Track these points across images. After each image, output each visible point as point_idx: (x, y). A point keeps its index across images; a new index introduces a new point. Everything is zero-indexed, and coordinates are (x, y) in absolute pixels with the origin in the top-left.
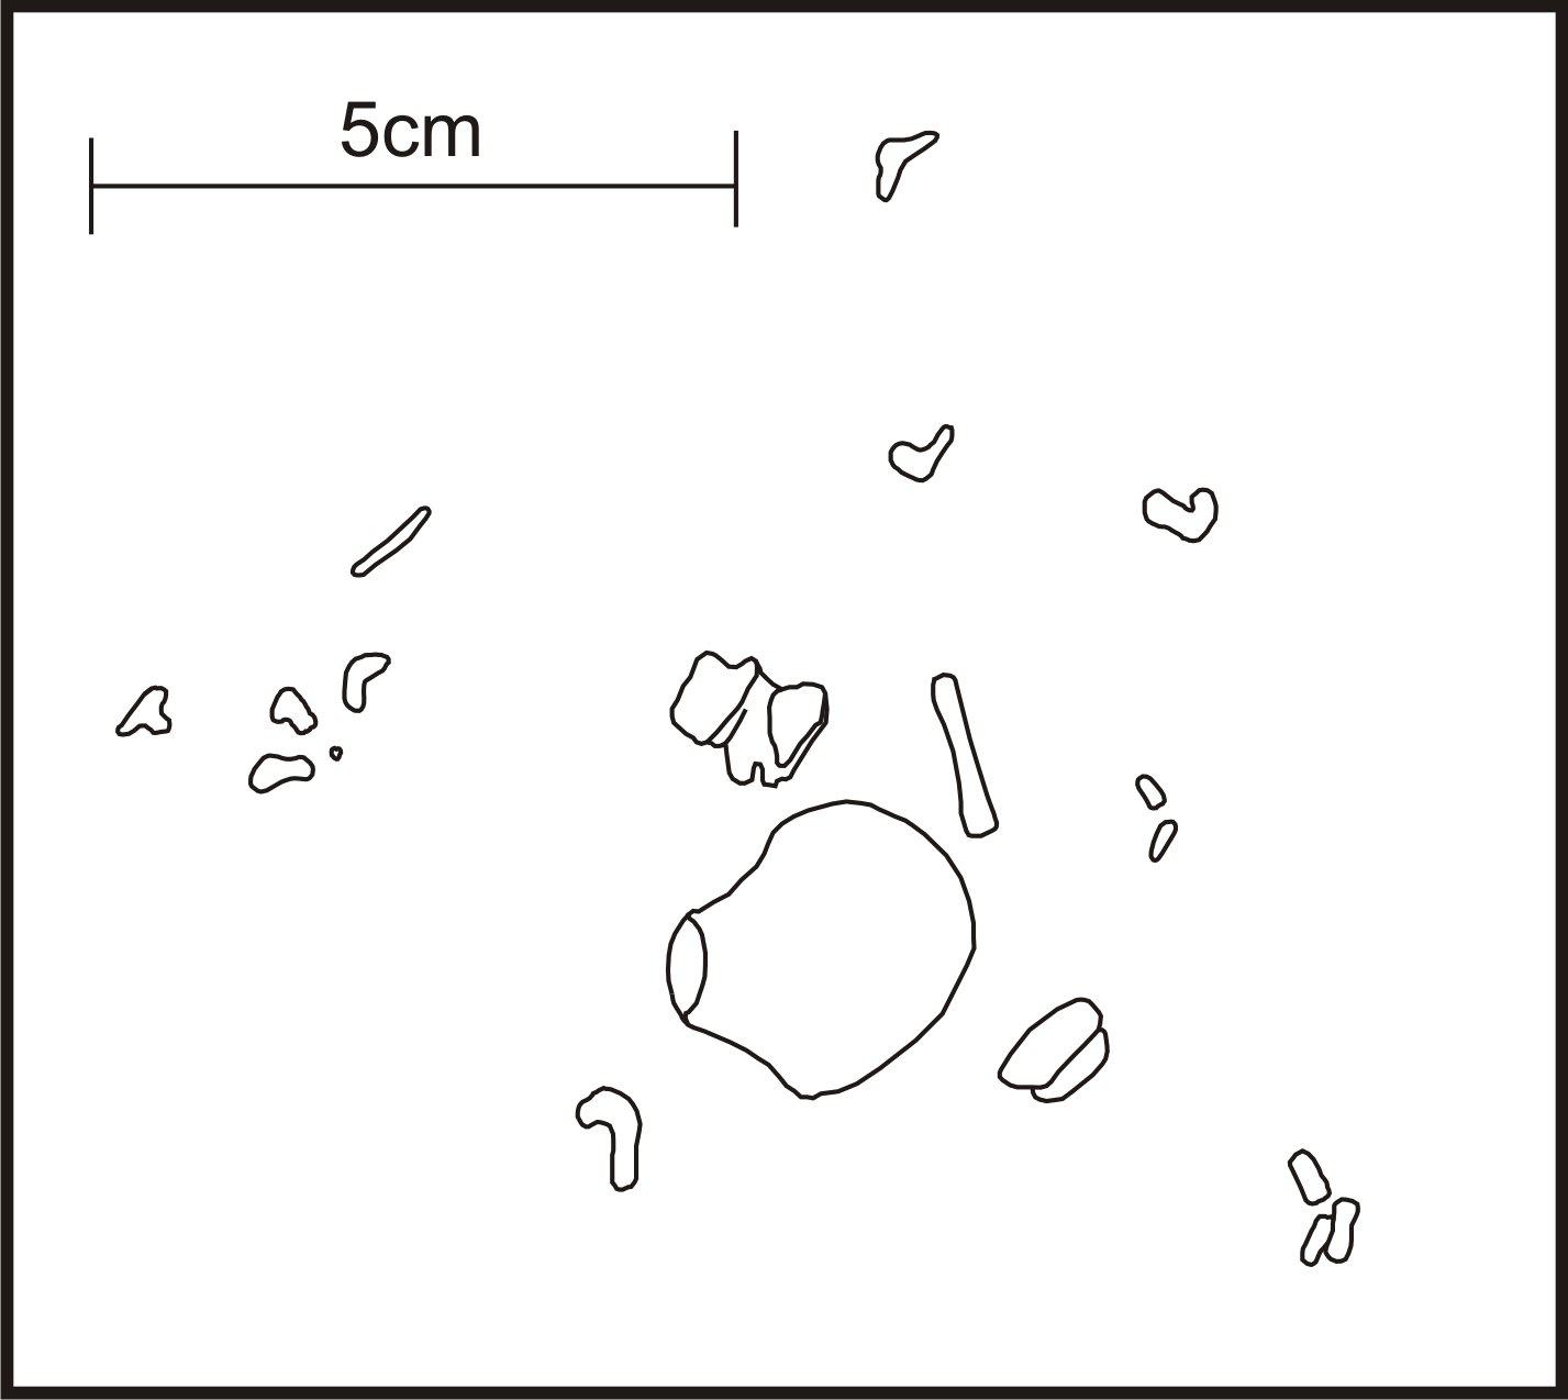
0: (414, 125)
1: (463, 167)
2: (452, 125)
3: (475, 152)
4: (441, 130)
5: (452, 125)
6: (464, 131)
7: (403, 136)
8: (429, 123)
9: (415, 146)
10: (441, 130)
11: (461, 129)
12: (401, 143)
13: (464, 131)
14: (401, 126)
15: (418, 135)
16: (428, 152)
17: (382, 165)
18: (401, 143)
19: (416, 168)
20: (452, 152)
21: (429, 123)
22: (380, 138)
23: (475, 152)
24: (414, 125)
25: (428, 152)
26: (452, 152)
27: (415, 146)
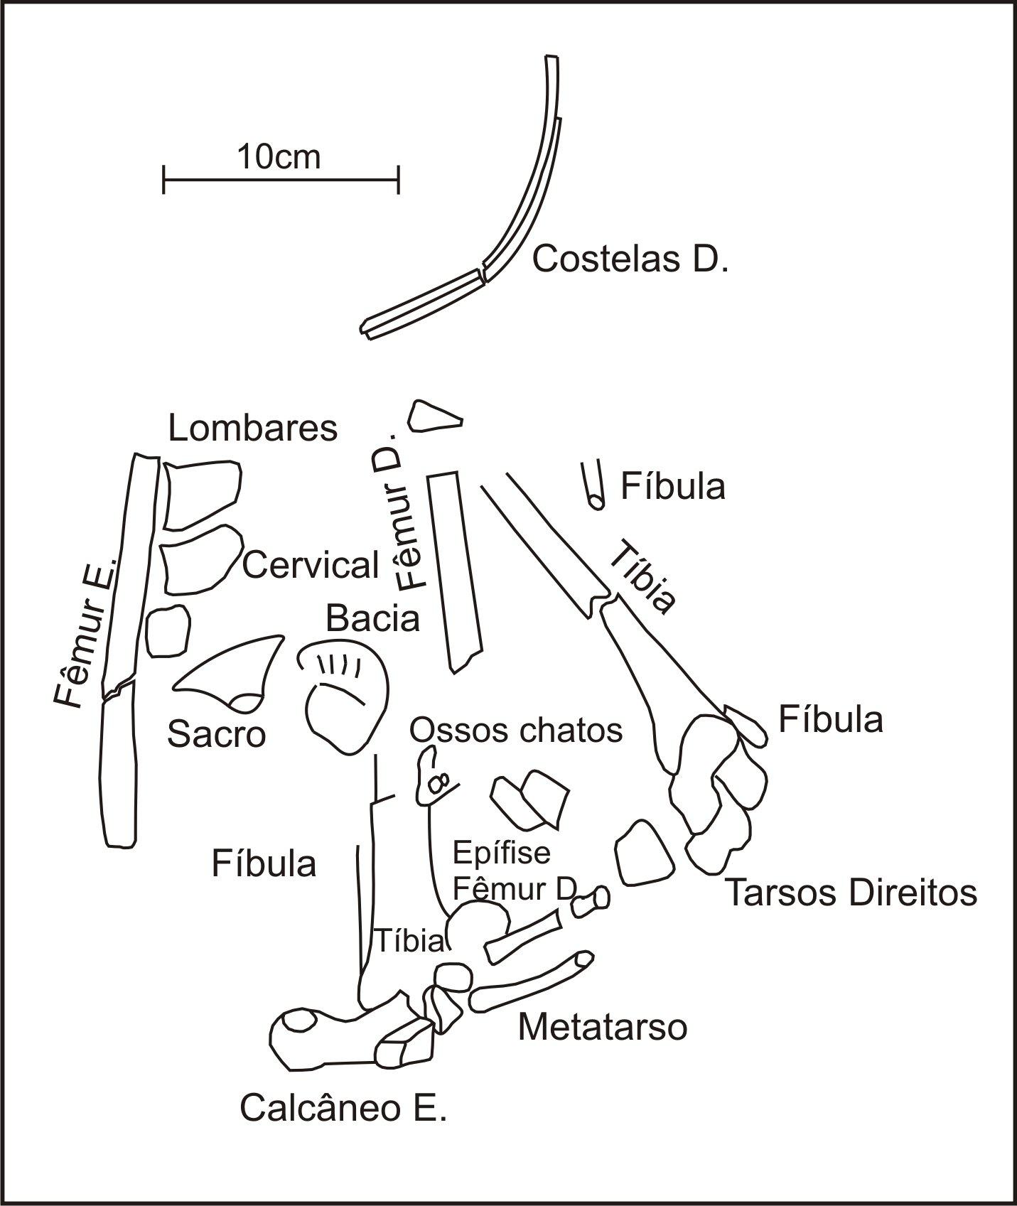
1: (312, 172)
2: (307, 154)
4: (302, 157)
5: (307, 154)
6: (313, 157)
7: (284, 159)
8: (297, 153)
10: (302, 157)
12: (283, 162)
13: (313, 157)
14: (284, 155)
15: (292, 159)
17: (273, 171)
18: (283, 162)
19: (291, 173)
21: (297, 153)
22: (275, 158)
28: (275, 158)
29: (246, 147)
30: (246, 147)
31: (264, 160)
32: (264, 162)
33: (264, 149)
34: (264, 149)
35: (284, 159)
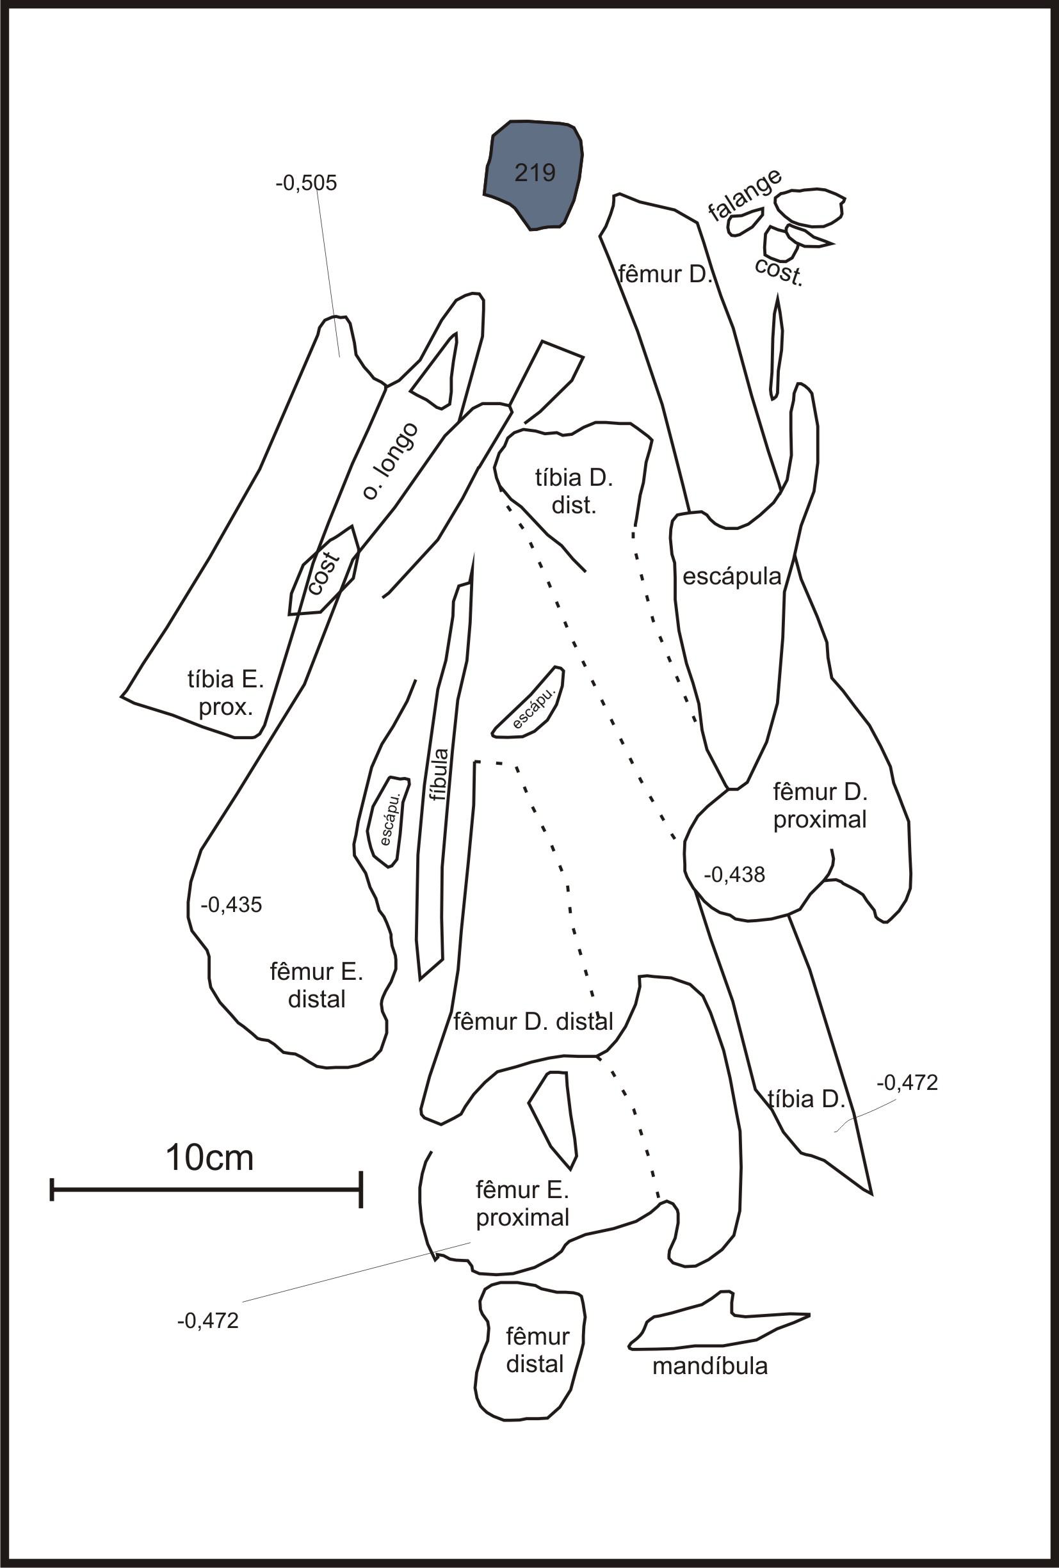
0: (221, 1155)
3: (251, 1168)
4: (234, 1157)
6: (245, 1158)
7: (216, 1160)
8: (228, 1154)
9: (221, 1165)
10: (234, 1157)
11: (243, 1157)
12: (215, 1164)
13: (245, 1158)
14: (214, 1156)
15: (223, 1160)
16: (228, 1168)
18: (215, 1164)
20: (239, 1168)
22: (205, 1159)
23: (251, 1168)
24: (221, 1155)
25: (228, 1168)
26: (239, 1168)
27: (221, 1165)
28: (205, 1159)
29: (175, 1147)
30: (175, 1147)
31: (195, 1160)
32: (194, 1162)
33: (194, 1151)
34: (194, 1151)
35: (216, 1160)
